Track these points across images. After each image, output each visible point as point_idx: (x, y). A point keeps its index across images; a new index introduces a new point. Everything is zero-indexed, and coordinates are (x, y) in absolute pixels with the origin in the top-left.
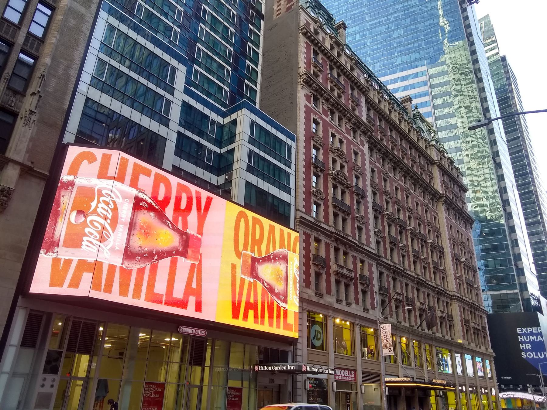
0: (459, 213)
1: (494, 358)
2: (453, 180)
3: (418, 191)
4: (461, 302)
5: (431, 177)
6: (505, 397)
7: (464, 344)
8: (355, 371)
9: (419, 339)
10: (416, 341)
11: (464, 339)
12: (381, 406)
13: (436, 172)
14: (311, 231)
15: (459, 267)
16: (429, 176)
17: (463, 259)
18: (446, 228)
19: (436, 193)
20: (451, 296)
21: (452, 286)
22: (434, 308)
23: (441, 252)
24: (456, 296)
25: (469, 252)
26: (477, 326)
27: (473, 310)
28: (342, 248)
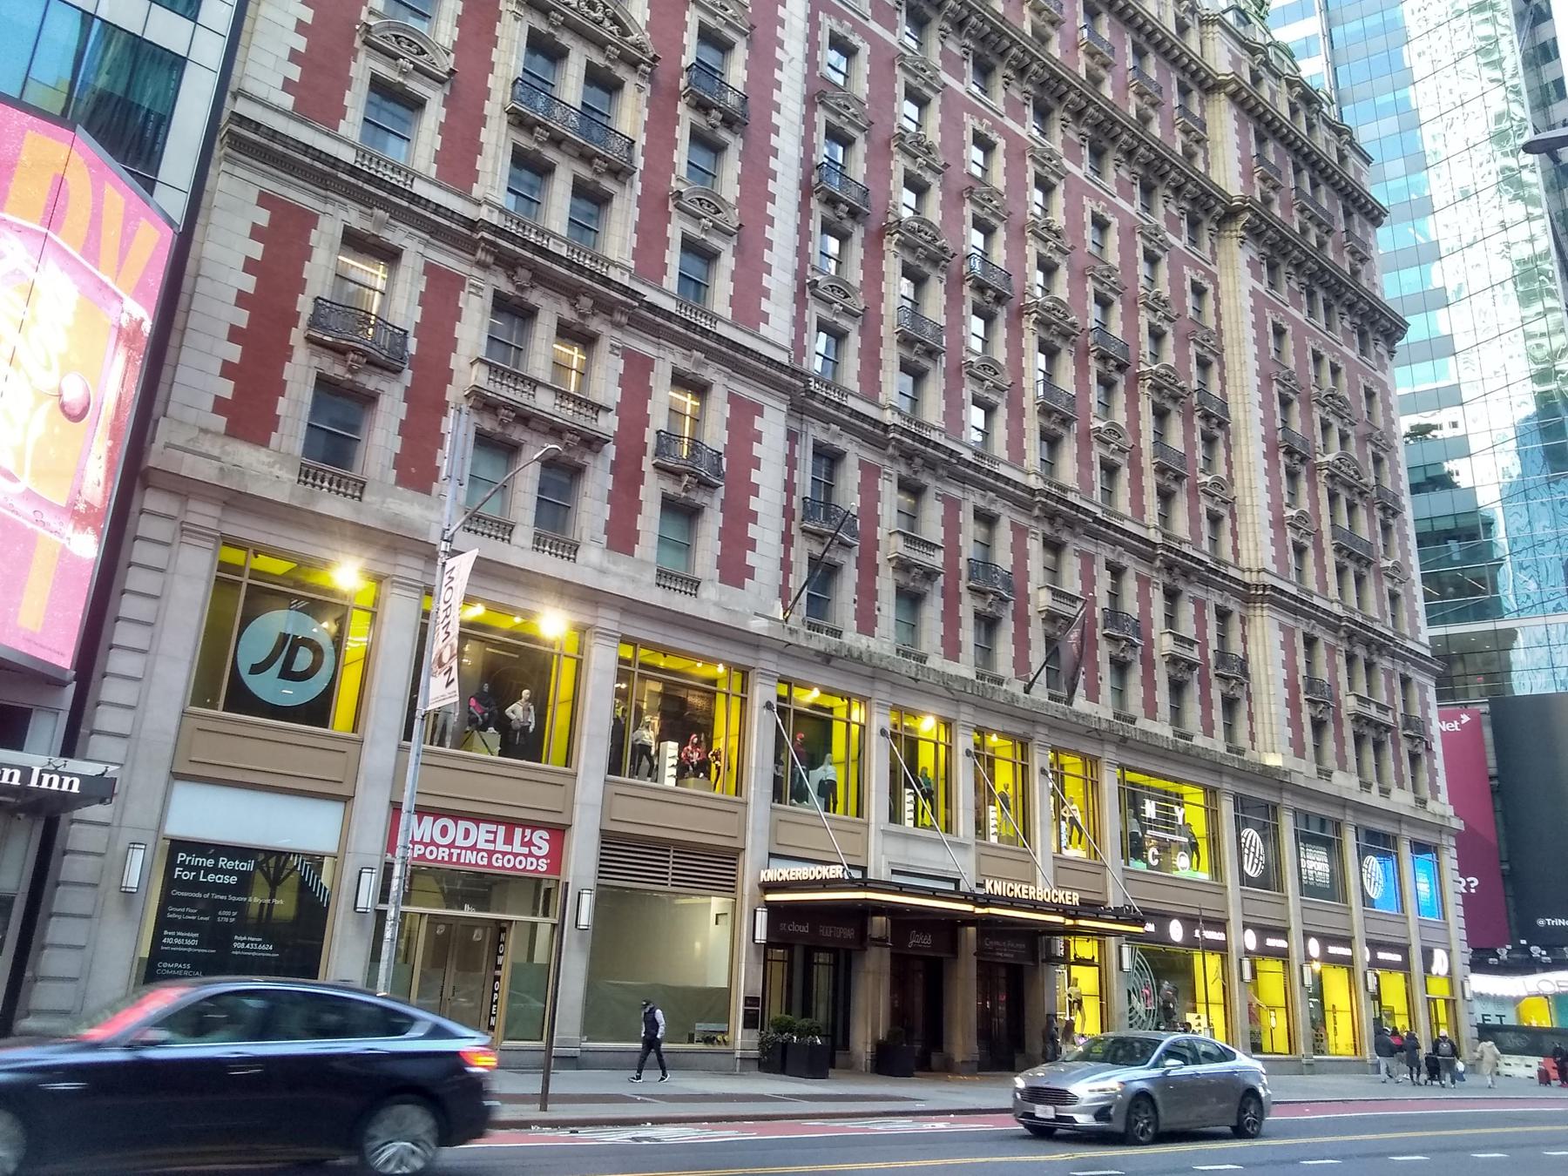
0: (1327, 288)
1: (1458, 836)
2: (1314, 165)
3: (1113, 173)
4: (1295, 611)
5: (1197, 135)
6: (1549, 988)
7: (1287, 773)
8: (558, 833)
9: (1019, 729)
10: (1003, 735)
11: (1299, 752)
12: (728, 991)
13: (1223, 121)
14: (326, 200)
15: (1304, 485)
16: (1186, 132)
17: (1330, 457)
18: (1250, 333)
19: (1210, 195)
20: (1247, 586)
21: (1255, 549)
22: (1141, 627)
23: (1215, 424)
24: (1265, 587)
25: (1366, 438)
26: (1373, 712)
27: (1361, 652)
28: (550, 311)
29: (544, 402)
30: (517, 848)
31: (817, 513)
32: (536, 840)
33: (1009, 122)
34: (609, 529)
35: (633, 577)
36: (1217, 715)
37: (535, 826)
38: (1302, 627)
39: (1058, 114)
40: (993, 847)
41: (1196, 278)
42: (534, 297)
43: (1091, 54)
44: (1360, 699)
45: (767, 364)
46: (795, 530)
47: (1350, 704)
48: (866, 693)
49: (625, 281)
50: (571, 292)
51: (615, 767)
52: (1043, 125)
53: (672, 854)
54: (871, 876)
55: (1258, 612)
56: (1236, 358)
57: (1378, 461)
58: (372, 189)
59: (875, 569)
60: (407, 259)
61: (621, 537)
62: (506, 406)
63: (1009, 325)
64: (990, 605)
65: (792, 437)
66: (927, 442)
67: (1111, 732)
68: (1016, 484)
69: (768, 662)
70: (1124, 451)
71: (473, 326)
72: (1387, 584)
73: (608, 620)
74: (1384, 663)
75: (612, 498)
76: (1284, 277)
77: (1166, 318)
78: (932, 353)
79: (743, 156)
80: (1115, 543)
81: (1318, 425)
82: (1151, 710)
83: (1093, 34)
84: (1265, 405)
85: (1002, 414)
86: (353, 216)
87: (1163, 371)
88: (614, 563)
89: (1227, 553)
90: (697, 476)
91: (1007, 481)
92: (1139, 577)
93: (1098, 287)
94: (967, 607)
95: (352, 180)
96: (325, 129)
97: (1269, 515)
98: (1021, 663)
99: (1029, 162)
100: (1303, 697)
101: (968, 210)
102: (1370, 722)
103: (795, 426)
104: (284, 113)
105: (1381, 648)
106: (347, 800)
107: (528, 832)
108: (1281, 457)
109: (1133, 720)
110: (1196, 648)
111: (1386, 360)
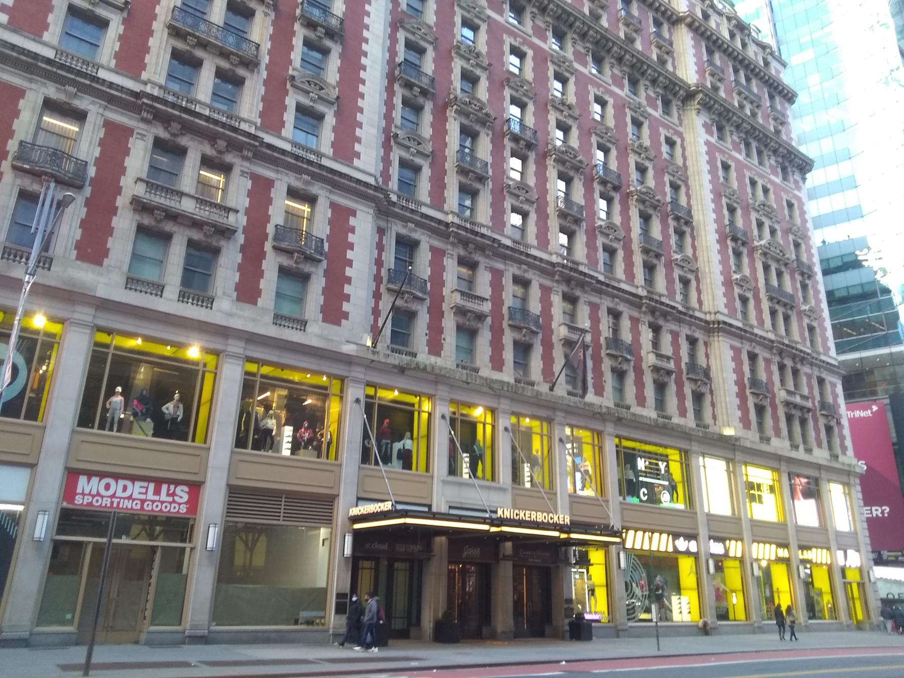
2: (747, 67)
4: (741, 338)
5: (667, 50)
7: (737, 439)
9: (543, 413)
10: (533, 417)
14: (31, 81)
15: (745, 260)
17: (762, 242)
18: (706, 168)
20: (707, 322)
21: (713, 299)
23: (684, 223)
24: (719, 323)
26: (798, 400)
27: (788, 363)
28: (196, 149)
29: (188, 206)
31: (398, 278)
33: (536, 41)
34: (239, 288)
35: (257, 319)
36: (689, 403)
38: (746, 347)
39: (570, 36)
40: (527, 490)
41: (668, 135)
42: (184, 141)
43: (627, 25)
44: (789, 392)
46: (382, 289)
47: (782, 395)
48: (432, 392)
49: (252, 130)
50: (212, 138)
51: (240, 442)
52: (561, 43)
53: (283, 500)
54: (434, 509)
55: (716, 338)
56: (697, 183)
57: (797, 245)
58: (63, 73)
59: (442, 314)
60: (90, 118)
61: (248, 292)
62: (158, 208)
63: (537, 162)
64: (524, 336)
65: (381, 232)
66: (477, 234)
67: (610, 414)
68: (541, 260)
69: (358, 373)
70: (620, 240)
71: (138, 159)
72: (806, 321)
73: (236, 347)
74: (805, 369)
75: (241, 268)
76: (728, 134)
77: (647, 158)
78: (481, 179)
79: (342, 56)
80: (614, 296)
81: (754, 223)
82: (641, 400)
83: (628, 13)
84: (717, 210)
85: (533, 217)
86: (52, 91)
87: (645, 190)
89: (694, 303)
90: (303, 253)
91: (535, 258)
92: (631, 318)
93: (600, 140)
94: (508, 338)
95: (49, 67)
96: (32, 36)
97: (722, 278)
98: (547, 372)
99: (549, 64)
100: (748, 391)
101: (507, 93)
102: (796, 406)
103: (383, 224)
105: (802, 360)
106: (32, 466)
108: (729, 242)
109: (628, 408)
110: (672, 362)
111: (801, 183)
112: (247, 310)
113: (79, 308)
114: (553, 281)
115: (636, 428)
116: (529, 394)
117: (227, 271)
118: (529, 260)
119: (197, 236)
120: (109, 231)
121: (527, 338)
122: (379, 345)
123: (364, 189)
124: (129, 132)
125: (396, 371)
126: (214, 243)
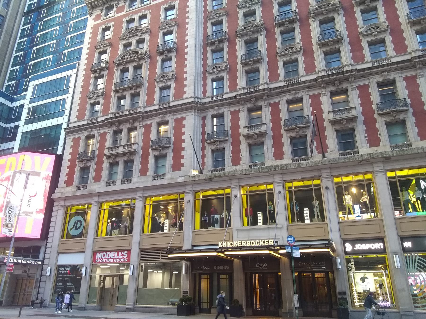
8: (129, 251)
28: (124, 128)
29: (121, 150)
30: (120, 257)
32: (124, 254)
35: (147, 181)
37: (124, 250)
45: (181, 106)
50: (127, 121)
53: (161, 251)
75: (141, 163)
86: (86, 133)
88: (141, 179)
103: (203, 115)
104: (76, 122)
107: (122, 252)
112: (144, 178)
113: (94, 198)
114: (321, 89)
115: (410, 159)
116: (292, 167)
117: (137, 167)
118: (295, 87)
119: (125, 158)
120: (101, 169)
121: (300, 133)
122: (204, 171)
123: (185, 106)
124: (106, 134)
125: (208, 181)
126: (132, 158)
